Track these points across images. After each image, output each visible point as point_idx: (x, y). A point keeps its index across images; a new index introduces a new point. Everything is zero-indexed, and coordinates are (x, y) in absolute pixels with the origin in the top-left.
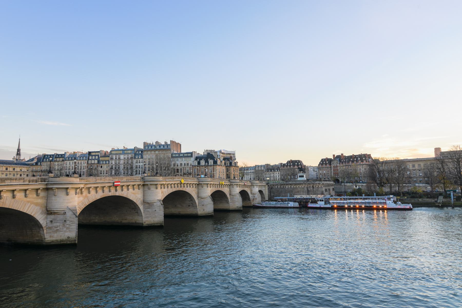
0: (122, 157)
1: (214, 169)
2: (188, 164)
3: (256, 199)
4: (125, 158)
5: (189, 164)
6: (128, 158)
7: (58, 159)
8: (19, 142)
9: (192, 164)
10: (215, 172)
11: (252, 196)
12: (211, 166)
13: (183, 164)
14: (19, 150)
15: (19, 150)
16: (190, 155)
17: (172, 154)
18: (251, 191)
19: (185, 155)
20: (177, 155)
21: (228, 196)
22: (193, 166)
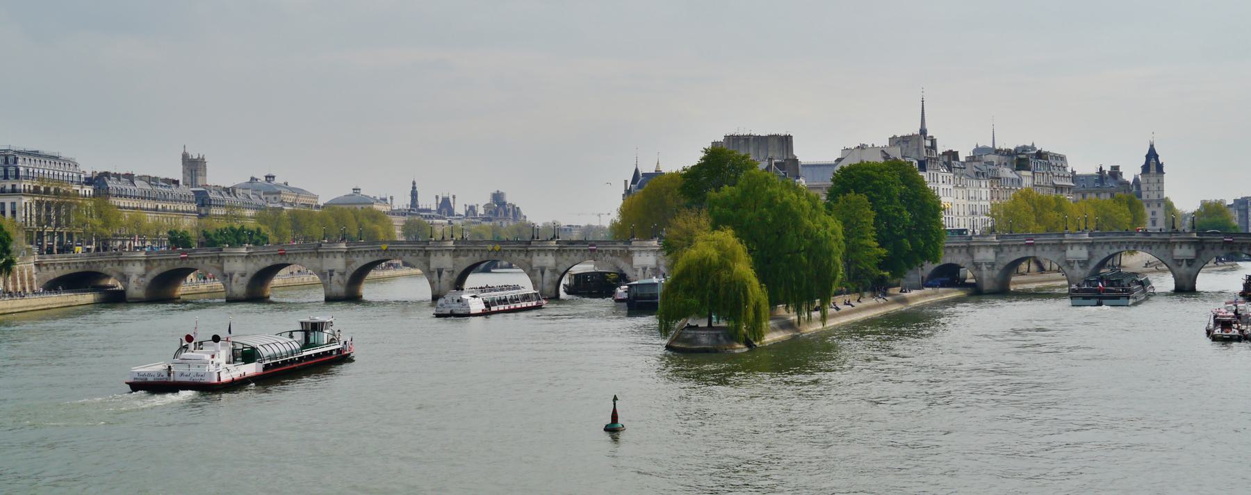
8: (923, 106)
18: (631, 263)
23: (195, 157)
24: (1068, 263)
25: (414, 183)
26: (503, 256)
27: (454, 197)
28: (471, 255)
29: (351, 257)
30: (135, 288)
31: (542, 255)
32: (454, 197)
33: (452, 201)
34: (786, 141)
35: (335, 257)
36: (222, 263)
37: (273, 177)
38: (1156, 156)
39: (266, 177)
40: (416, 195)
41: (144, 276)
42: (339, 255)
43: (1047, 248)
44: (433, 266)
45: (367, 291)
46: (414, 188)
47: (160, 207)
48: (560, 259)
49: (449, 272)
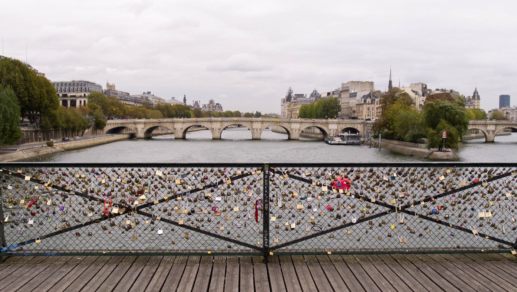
14: (390, 82)
23: (111, 84)
24: (488, 131)
25: (185, 96)
27: (200, 101)
28: (268, 123)
30: (141, 134)
32: (200, 101)
33: (199, 103)
34: (372, 83)
36: (174, 124)
37: (150, 92)
38: (477, 93)
39: (148, 92)
40: (186, 100)
41: (144, 129)
42: (219, 122)
43: (480, 126)
44: (254, 127)
45: (188, 136)
46: (185, 98)
47: (125, 103)
48: (301, 126)
49: (260, 129)
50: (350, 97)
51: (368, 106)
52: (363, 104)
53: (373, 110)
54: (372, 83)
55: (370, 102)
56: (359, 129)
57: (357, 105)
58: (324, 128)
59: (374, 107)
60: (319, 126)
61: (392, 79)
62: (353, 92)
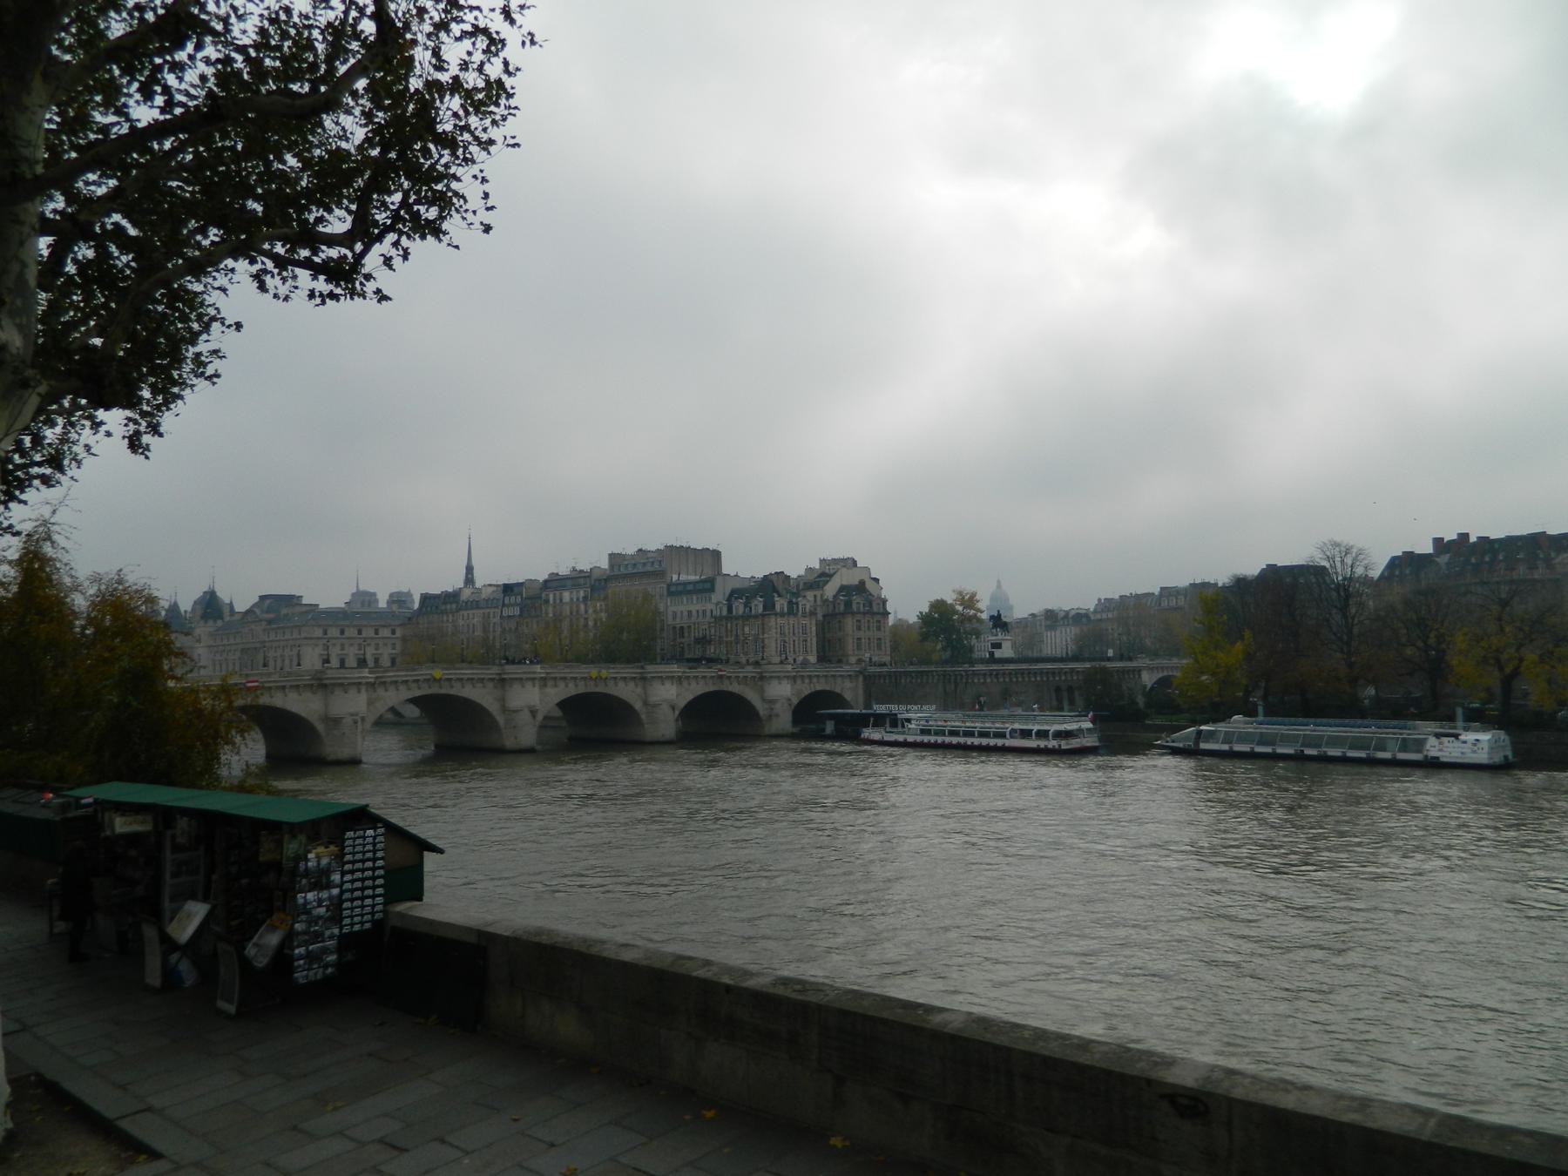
0: (566, 596)
1: (763, 624)
2: (704, 612)
3: (777, 715)
4: (572, 599)
5: (708, 613)
6: (578, 599)
7: (448, 607)
9: (714, 613)
10: (766, 636)
11: (766, 706)
12: (756, 617)
13: (694, 613)
14: (470, 569)
15: (470, 569)
16: (708, 586)
17: (669, 586)
18: (762, 691)
19: (700, 586)
20: (680, 588)
21: (638, 706)
22: (715, 618)
26: (606, 685)
28: (562, 685)
29: (375, 691)
31: (668, 685)
34: (716, 555)
35: (359, 692)
42: (363, 689)
50: (670, 594)
51: (779, 620)
52: (763, 616)
53: (794, 634)
54: (716, 555)
55: (786, 610)
56: (848, 696)
57: (718, 619)
58: (752, 696)
59: (796, 626)
60: (735, 688)
61: (474, 563)
62: (675, 578)
